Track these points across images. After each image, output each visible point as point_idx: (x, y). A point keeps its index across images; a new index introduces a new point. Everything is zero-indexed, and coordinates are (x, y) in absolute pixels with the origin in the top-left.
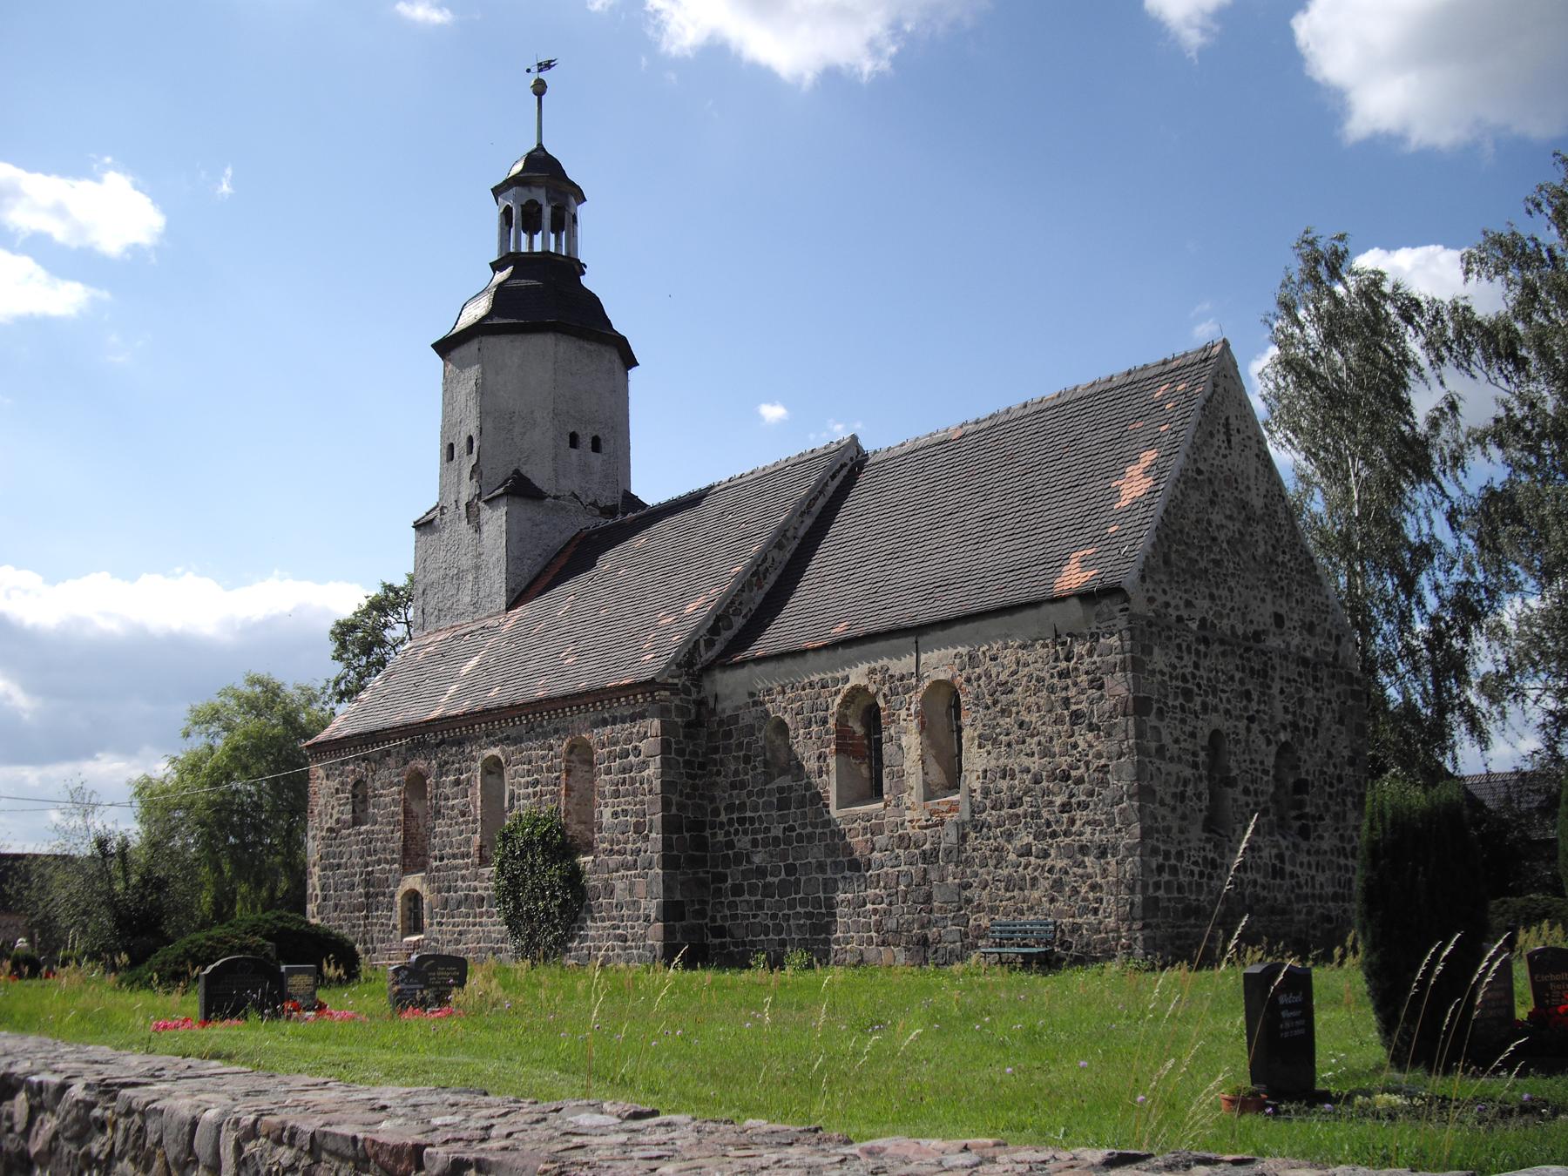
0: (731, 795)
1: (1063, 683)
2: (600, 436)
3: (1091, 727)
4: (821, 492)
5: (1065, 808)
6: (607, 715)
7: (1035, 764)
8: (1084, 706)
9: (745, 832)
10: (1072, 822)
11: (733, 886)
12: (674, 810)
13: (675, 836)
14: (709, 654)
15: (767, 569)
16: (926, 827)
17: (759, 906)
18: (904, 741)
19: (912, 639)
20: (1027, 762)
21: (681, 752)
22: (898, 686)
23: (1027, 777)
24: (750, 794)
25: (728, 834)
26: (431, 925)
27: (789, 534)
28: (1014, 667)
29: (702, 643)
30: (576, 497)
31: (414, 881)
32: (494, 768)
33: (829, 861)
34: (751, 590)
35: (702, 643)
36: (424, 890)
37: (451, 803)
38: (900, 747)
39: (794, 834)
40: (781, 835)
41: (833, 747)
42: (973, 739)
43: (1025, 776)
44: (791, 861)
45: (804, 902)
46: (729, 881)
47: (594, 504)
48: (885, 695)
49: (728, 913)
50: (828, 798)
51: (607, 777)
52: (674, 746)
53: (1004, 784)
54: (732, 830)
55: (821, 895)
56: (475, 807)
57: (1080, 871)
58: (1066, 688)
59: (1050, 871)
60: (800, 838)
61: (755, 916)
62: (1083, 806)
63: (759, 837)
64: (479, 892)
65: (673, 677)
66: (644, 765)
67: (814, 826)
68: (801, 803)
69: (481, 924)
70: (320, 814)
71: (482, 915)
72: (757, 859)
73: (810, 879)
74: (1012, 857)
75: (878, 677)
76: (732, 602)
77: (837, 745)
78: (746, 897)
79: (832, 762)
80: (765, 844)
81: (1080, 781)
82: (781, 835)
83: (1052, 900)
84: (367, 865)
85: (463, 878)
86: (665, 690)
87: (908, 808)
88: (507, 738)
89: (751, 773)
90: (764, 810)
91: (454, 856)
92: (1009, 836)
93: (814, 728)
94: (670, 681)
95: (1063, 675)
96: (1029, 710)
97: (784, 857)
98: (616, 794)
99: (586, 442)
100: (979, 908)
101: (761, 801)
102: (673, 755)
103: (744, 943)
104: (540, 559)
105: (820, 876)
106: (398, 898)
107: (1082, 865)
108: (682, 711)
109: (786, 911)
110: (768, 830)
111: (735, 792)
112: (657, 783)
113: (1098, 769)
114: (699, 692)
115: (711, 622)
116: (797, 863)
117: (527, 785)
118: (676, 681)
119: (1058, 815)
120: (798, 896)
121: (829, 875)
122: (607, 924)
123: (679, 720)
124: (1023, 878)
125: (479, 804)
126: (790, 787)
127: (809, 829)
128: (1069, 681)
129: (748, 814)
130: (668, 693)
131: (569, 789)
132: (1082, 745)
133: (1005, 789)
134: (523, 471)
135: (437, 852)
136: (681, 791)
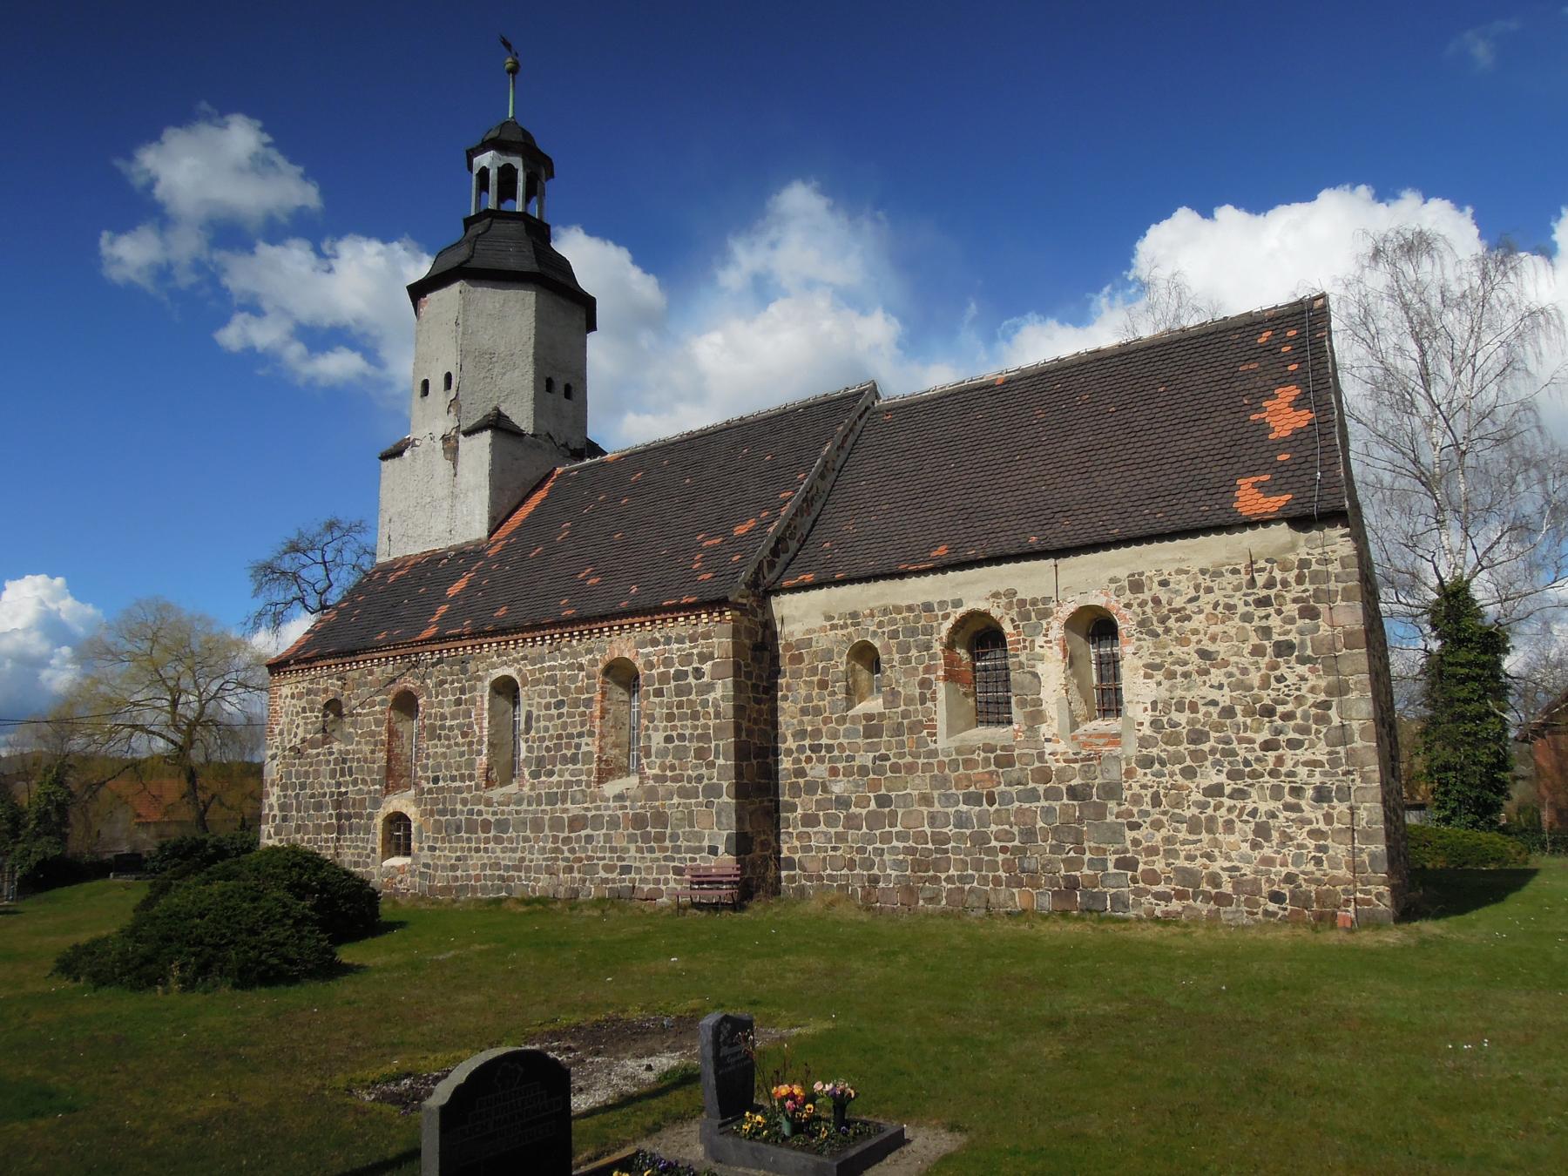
0: (801, 722)
1: (1262, 612)
2: (572, 384)
3: (1302, 660)
4: (851, 430)
5: (1268, 746)
6: (657, 635)
7: (1224, 698)
8: (1294, 637)
9: (821, 760)
10: (1280, 761)
11: (805, 816)
12: (744, 737)
13: (745, 764)
14: (771, 575)
15: (813, 498)
16: (1076, 761)
17: (841, 837)
18: (1040, 668)
19: (1052, 561)
20: (1214, 694)
21: (749, 675)
22: (1033, 611)
23: (1214, 711)
24: (826, 721)
25: (797, 761)
26: (421, 849)
27: (829, 465)
28: (1192, 593)
29: (765, 564)
30: (551, 437)
31: (401, 802)
32: (506, 690)
33: (936, 793)
34: (802, 516)
35: (765, 564)
36: (412, 812)
37: (448, 723)
38: (1035, 675)
39: (888, 764)
40: (870, 765)
41: (941, 673)
42: (1137, 669)
43: (1211, 709)
44: (883, 791)
45: (902, 837)
46: (799, 810)
47: (565, 445)
48: (1012, 620)
49: (797, 844)
50: (935, 727)
51: (657, 700)
52: (743, 669)
53: (1182, 718)
54: (803, 757)
55: (928, 830)
56: (481, 728)
57: (1293, 815)
58: (1267, 617)
59: (1254, 813)
60: (895, 768)
61: (834, 849)
62: (1294, 744)
63: (840, 766)
64: (485, 816)
65: (742, 597)
66: (710, 687)
67: (916, 756)
68: (898, 730)
69: (486, 850)
70: (281, 733)
71: (487, 841)
72: (837, 789)
73: (911, 812)
74: (1197, 796)
75: (1004, 601)
76: (789, 526)
77: (946, 671)
78: (822, 827)
79: (941, 689)
80: (848, 772)
81: (1288, 716)
82: (870, 765)
83: (1255, 846)
84: (339, 785)
85: (464, 802)
86: (736, 609)
87: (1048, 740)
89: (828, 698)
90: (845, 736)
91: (453, 779)
92: (1189, 773)
93: (914, 653)
94: (740, 600)
95: (1263, 602)
96: (1213, 639)
97: (874, 786)
98: (670, 717)
99: (560, 388)
100: (1152, 851)
101: (841, 728)
102: (743, 679)
103: (821, 878)
104: (518, 491)
105: (925, 810)
106: (379, 821)
107: (1295, 808)
108: (751, 633)
109: (878, 845)
110: (851, 758)
111: (806, 719)
112: (727, 707)
113: (1316, 705)
114: (763, 614)
115: (772, 544)
116: (893, 794)
117: (548, 707)
118: (744, 601)
119: (1260, 753)
120: (894, 830)
121: (937, 807)
122: (657, 855)
123: (747, 642)
124: (1212, 819)
125: (486, 724)
126: (882, 715)
127: (909, 759)
128: (1271, 610)
129: (824, 741)
130: (738, 613)
131: (604, 712)
132: (1292, 679)
133: (1183, 722)
134: (502, 409)
135: (429, 773)
136: (749, 715)
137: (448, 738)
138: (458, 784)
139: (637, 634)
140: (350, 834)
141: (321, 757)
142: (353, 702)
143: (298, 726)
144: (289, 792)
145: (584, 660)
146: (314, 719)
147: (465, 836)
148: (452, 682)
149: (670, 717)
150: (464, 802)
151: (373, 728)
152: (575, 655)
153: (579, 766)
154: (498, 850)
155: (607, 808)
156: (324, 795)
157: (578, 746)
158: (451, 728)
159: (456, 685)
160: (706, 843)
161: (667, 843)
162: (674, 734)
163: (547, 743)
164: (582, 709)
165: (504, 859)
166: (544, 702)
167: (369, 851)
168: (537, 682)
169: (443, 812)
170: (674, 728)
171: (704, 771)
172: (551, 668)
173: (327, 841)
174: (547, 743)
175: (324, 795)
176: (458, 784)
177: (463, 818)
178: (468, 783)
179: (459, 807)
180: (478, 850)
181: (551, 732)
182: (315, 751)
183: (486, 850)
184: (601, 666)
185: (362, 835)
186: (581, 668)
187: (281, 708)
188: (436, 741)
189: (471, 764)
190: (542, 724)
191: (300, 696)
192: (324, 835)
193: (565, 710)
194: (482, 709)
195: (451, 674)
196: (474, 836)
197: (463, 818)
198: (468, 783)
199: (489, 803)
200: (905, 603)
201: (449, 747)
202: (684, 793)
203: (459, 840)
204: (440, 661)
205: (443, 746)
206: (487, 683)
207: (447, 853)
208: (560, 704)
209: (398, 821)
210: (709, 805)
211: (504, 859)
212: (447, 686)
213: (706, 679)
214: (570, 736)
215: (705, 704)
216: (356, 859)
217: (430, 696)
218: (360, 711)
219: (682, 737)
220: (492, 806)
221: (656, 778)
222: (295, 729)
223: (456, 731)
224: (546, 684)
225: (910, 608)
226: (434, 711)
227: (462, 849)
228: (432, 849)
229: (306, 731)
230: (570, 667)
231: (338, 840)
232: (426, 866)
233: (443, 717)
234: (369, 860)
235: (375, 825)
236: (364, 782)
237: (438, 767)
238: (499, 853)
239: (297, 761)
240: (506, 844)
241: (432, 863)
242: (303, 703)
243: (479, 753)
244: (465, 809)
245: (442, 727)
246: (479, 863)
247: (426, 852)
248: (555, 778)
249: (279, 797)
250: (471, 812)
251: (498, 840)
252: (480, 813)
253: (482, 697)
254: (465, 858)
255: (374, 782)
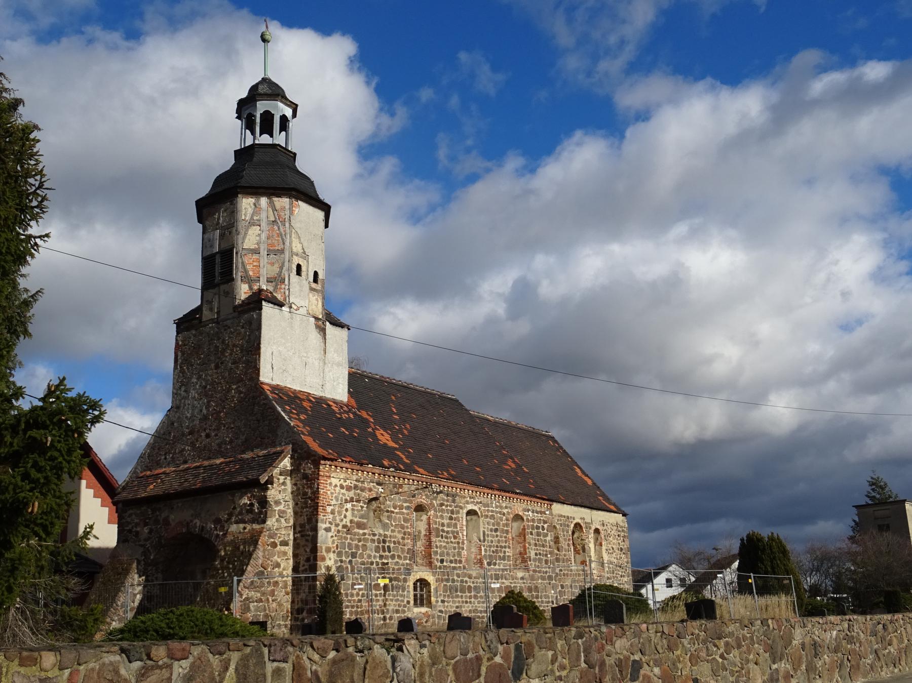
26: (437, 602)
36: (431, 579)
51: (531, 536)
56: (463, 535)
66: (546, 535)
70: (333, 512)
71: (470, 597)
85: (458, 576)
88: (481, 503)
91: (451, 562)
106: (411, 584)
116: (564, 584)
117: (491, 530)
127: (566, 572)
137: (447, 538)
138: (453, 565)
139: (524, 506)
140: (393, 591)
141: (367, 536)
142: (388, 502)
143: (347, 510)
144: (344, 558)
145: (505, 511)
146: (360, 508)
147: (460, 594)
148: (447, 506)
149: (536, 545)
150: (458, 576)
151: (402, 523)
152: (501, 507)
153: (506, 562)
154: (476, 602)
155: (518, 583)
156: (372, 563)
157: (505, 552)
158: (448, 532)
159: (449, 508)
160: (550, 600)
161: (540, 600)
162: (538, 552)
163: (492, 549)
164: (505, 535)
165: (479, 607)
166: (490, 527)
167: (405, 603)
168: (487, 516)
169: (447, 580)
170: (537, 549)
171: (548, 570)
172: (492, 511)
173: (376, 595)
174: (492, 549)
175: (372, 563)
176: (453, 565)
177: (459, 584)
178: (458, 565)
179: (456, 578)
180: (466, 602)
181: (494, 543)
182: (361, 532)
183: (470, 602)
184: (512, 516)
185: (400, 592)
186: (504, 514)
187: (332, 493)
188: (440, 538)
189: (459, 554)
190: (490, 539)
191: (349, 489)
192: (374, 592)
193: (498, 533)
194: (463, 525)
195: (447, 501)
196: (464, 595)
197: (459, 584)
198: (458, 565)
199: (470, 577)
200: (566, 515)
201: (447, 543)
202: (543, 578)
203: (457, 596)
204: (441, 492)
205: (444, 542)
206: (465, 511)
207: (451, 603)
208: (496, 530)
209: (422, 583)
210: (550, 584)
211: (479, 607)
212: (444, 507)
213: (545, 531)
214: (501, 547)
215: (545, 541)
216: (397, 608)
217: (435, 511)
218: (392, 509)
219: (540, 554)
220: (471, 578)
221: (534, 571)
222: (344, 512)
223: (451, 535)
224: (491, 519)
225: (564, 517)
226: (438, 520)
227: (459, 602)
228: (443, 601)
229: (353, 515)
230: (500, 513)
231: (385, 596)
232: (441, 611)
233: (443, 525)
234: (406, 609)
235: (408, 586)
236: (399, 557)
237: (442, 554)
238: (476, 604)
239: (349, 536)
240: (479, 599)
241: (444, 610)
242: (351, 494)
243: (463, 549)
244: (459, 579)
245: (443, 531)
246: (468, 609)
247: (440, 603)
248: (497, 567)
249: (336, 562)
250: (462, 581)
251: (476, 597)
252: (466, 582)
253: (462, 518)
254: (461, 606)
255: (405, 558)
